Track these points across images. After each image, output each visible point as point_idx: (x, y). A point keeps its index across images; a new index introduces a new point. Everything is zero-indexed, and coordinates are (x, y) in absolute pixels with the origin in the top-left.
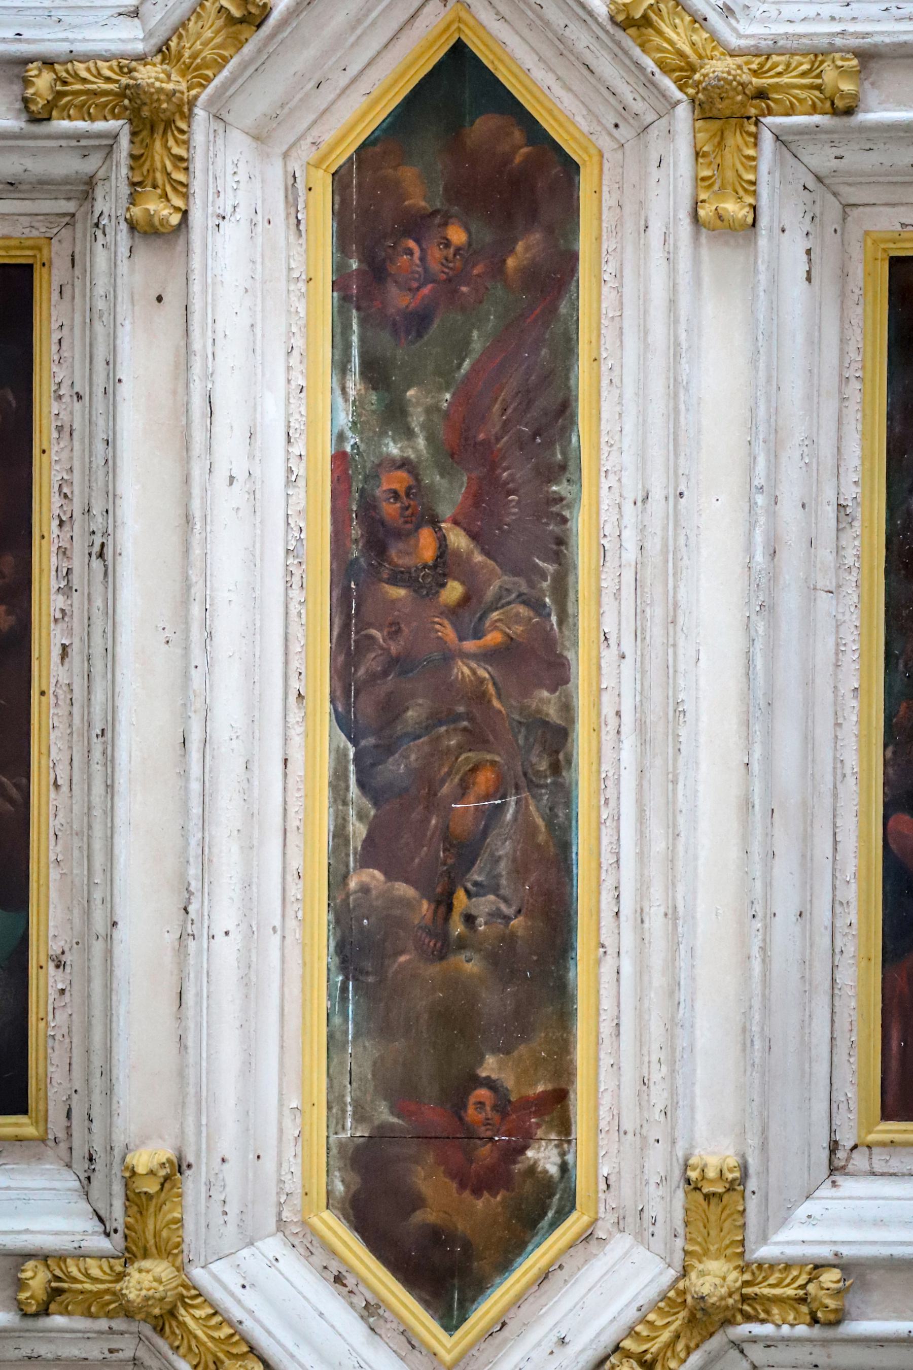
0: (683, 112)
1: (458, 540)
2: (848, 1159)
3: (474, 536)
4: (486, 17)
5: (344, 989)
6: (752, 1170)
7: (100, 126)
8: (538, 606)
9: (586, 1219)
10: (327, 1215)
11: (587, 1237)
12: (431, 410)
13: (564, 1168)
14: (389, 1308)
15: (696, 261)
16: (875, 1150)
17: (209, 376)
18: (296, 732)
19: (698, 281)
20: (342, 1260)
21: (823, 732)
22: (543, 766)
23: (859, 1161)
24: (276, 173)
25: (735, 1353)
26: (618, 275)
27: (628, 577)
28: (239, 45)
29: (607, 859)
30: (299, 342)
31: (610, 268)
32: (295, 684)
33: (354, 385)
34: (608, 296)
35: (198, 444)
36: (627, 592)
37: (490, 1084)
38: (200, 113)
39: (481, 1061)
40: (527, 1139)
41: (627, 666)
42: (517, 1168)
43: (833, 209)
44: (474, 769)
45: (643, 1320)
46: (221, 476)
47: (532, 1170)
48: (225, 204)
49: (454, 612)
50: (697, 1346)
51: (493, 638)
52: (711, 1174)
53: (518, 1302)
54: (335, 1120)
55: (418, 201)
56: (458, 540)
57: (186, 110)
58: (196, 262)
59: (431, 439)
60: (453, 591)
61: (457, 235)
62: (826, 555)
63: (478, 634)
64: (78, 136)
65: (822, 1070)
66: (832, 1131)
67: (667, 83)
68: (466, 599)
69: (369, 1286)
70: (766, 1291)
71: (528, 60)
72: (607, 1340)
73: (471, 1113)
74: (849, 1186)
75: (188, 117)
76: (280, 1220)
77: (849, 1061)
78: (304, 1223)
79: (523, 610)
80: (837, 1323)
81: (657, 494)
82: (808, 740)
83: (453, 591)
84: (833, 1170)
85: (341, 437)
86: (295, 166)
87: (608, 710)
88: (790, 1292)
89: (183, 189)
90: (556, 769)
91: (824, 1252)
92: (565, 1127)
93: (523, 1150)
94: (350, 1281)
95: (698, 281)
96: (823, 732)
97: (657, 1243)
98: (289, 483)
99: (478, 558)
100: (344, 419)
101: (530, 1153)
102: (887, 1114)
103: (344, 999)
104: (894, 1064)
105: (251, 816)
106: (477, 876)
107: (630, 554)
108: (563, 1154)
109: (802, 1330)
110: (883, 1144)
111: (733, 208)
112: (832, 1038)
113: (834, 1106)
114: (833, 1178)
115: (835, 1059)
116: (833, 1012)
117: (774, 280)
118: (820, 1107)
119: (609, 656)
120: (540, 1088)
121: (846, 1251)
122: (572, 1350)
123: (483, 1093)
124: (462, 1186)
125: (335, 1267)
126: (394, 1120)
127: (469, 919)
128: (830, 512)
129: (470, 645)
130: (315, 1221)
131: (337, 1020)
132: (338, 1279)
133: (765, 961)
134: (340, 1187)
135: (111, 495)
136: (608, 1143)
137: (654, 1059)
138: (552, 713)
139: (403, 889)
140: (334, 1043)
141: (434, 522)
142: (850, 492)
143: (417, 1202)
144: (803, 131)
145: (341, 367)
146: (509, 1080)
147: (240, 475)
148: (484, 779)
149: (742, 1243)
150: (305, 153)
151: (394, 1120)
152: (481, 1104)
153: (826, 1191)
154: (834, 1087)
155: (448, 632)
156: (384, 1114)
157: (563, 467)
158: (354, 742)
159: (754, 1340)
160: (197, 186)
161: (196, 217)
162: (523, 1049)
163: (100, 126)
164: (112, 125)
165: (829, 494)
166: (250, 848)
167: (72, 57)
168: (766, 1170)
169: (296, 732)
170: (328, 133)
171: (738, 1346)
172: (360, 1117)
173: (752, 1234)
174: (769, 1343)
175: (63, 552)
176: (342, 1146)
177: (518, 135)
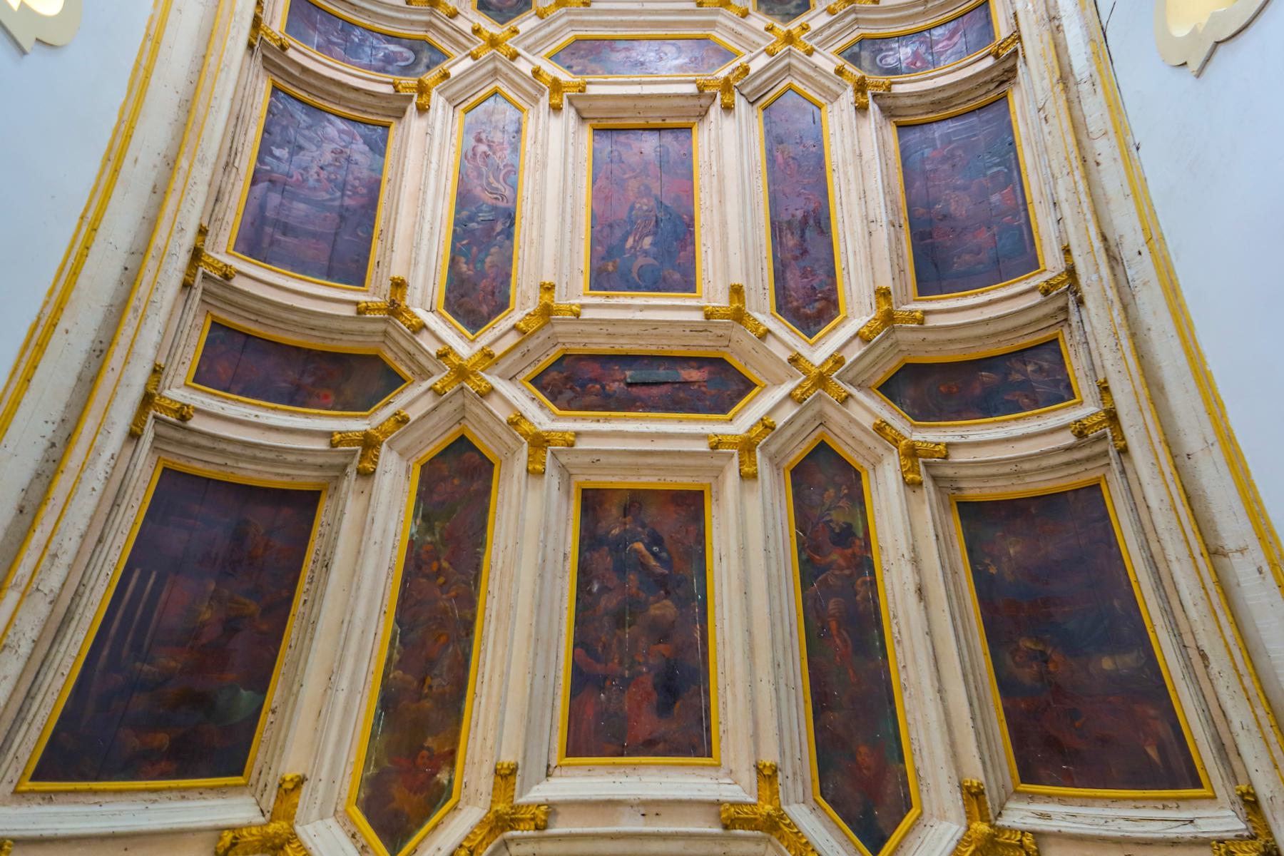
0: (526, 445)
1: (445, 564)
3: (451, 564)
4: (471, 428)
6: (520, 766)
7: (353, 448)
8: (469, 585)
11: (455, 808)
12: (443, 528)
15: (527, 482)
17: (374, 512)
18: (381, 625)
19: (527, 487)
21: (556, 619)
22: (463, 634)
24: (404, 464)
26: (503, 491)
27: (498, 573)
28: (399, 428)
29: (481, 663)
30: (403, 509)
31: (500, 490)
32: (384, 609)
33: (418, 521)
34: (500, 497)
35: (366, 531)
36: (498, 577)
38: (384, 444)
41: (495, 600)
43: (566, 475)
44: (440, 636)
46: (372, 541)
47: (438, 783)
48: (388, 469)
49: (441, 586)
51: (453, 593)
52: (505, 766)
55: (446, 473)
56: (445, 564)
57: (380, 444)
58: (376, 481)
59: (441, 535)
60: (441, 580)
61: (456, 482)
62: (560, 567)
63: (448, 592)
64: (345, 451)
65: (546, 737)
67: (522, 439)
68: (445, 582)
70: (519, 816)
71: (483, 438)
72: (457, 843)
74: (551, 780)
75: (381, 445)
79: (463, 585)
80: (545, 828)
81: (510, 545)
82: (551, 620)
83: (441, 580)
85: (412, 536)
86: (410, 463)
87: (487, 614)
88: (528, 816)
89: (375, 463)
90: (467, 635)
91: (542, 800)
93: (434, 775)
95: (527, 487)
96: (556, 619)
98: (394, 547)
99: (451, 570)
100: (414, 530)
105: (361, 648)
106: (436, 672)
107: (500, 565)
109: (532, 833)
111: (539, 467)
117: (549, 488)
119: (489, 598)
121: (550, 799)
127: (430, 687)
128: (562, 555)
129: (444, 596)
133: (531, 689)
135: (334, 547)
138: (469, 617)
139: (409, 677)
141: (438, 559)
142: (568, 550)
144: (559, 451)
145: (415, 516)
147: (378, 541)
148: (443, 639)
149: (513, 796)
150: (414, 460)
155: (438, 592)
157: (481, 544)
158: (400, 627)
160: (380, 462)
161: (378, 470)
163: (353, 448)
164: (356, 448)
165: (562, 549)
166: (357, 661)
167: (348, 431)
168: (524, 768)
169: (381, 625)
170: (421, 455)
173: (516, 793)
175: (313, 571)
177: (477, 457)
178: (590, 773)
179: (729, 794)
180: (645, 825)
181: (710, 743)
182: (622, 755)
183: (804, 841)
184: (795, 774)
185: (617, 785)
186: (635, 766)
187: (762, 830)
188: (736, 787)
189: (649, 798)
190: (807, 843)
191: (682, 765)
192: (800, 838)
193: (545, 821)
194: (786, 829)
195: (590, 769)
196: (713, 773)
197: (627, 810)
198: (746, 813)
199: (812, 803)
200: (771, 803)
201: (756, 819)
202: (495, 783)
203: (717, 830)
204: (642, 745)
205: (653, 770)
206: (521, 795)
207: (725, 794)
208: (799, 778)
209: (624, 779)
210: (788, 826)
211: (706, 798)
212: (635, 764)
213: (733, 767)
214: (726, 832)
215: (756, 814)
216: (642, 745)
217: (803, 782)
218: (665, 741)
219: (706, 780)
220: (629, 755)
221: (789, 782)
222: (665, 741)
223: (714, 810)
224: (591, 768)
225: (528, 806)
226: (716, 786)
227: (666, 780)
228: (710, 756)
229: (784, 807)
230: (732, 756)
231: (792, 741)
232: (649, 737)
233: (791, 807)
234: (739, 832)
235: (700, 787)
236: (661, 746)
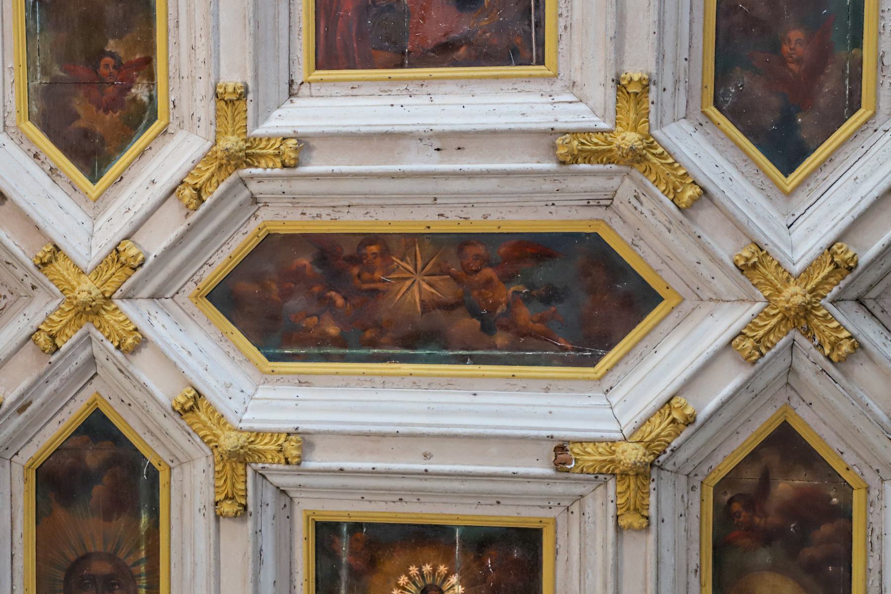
2: (299, 89)
5: (34, 6)
9: (163, 123)
10: (29, 123)
13: (152, 98)
14: (63, 170)
16: (312, 84)
20: (38, 146)
23: (305, 90)
25: (241, 186)
37: (112, 55)
39: (107, 42)
40: (131, 83)
42: (128, 98)
45: (194, 168)
50: (223, 180)
53: (129, 166)
54: (31, 76)
65: (284, 42)
66: (290, 75)
69: (52, 159)
73: (102, 70)
76: (5, 125)
77: (298, 38)
78: (17, 127)
84: (291, 95)
92: (151, 77)
94: (42, 157)
97: (202, 131)
101: (133, 90)
102: (317, 68)
103: (34, 12)
104: (321, 47)
108: (150, 91)
110: (317, 81)
112: (290, 26)
113: (291, 62)
114: (291, 99)
115: (291, 37)
116: (290, 13)
118: (284, 62)
120: (138, 57)
122: (158, 186)
123: (108, 59)
124: (98, 108)
125: (34, 150)
126: (62, 74)
130: (23, 126)
131: (31, 22)
132: (36, 156)
134: (35, 109)
136: (174, 83)
137: (198, 35)
140: (30, 34)
143: (77, 117)
146: (121, 52)
151: (62, 74)
152: (107, 65)
153: (288, 104)
154: (291, 52)
156: (57, 71)
159: (252, 177)
162: (128, 36)
171: (243, 181)
172: (45, 72)
174: (260, 179)
176: (36, 90)
178: (355, 92)
179: (569, 118)
180: (441, 162)
181: (541, 44)
182: (401, 66)
183: (682, 172)
184: (677, 82)
185: (397, 108)
186: (422, 82)
187: (618, 163)
188: (582, 107)
189: (447, 128)
190: (686, 174)
191: (497, 78)
192: (676, 169)
193: (296, 159)
194: (655, 160)
195: (355, 86)
196: (546, 87)
197: (413, 144)
198: (596, 144)
199: (702, 120)
200: (635, 129)
201: (611, 150)
202: (217, 110)
203: (550, 166)
204: (433, 51)
205: (450, 87)
206: (257, 125)
207: (562, 118)
208: (682, 86)
209: (406, 100)
210: (660, 156)
211: (533, 126)
212: (424, 79)
213: (577, 77)
214: (564, 168)
215: (610, 144)
216: (433, 51)
217: (688, 91)
218: (470, 44)
219: (535, 98)
220: (411, 66)
221: (667, 96)
222: (470, 44)
223: (546, 140)
224: (355, 84)
225: (269, 139)
226: (550, 107)
227: (469, 100)
228: (541, 61)
229: (656, 133)
230: (577, 62)
231: (677, 35)
232: (444, 40)
233: (665, 129)
234: (583, 166)
235: (525, 109)
236: (462, 51)
